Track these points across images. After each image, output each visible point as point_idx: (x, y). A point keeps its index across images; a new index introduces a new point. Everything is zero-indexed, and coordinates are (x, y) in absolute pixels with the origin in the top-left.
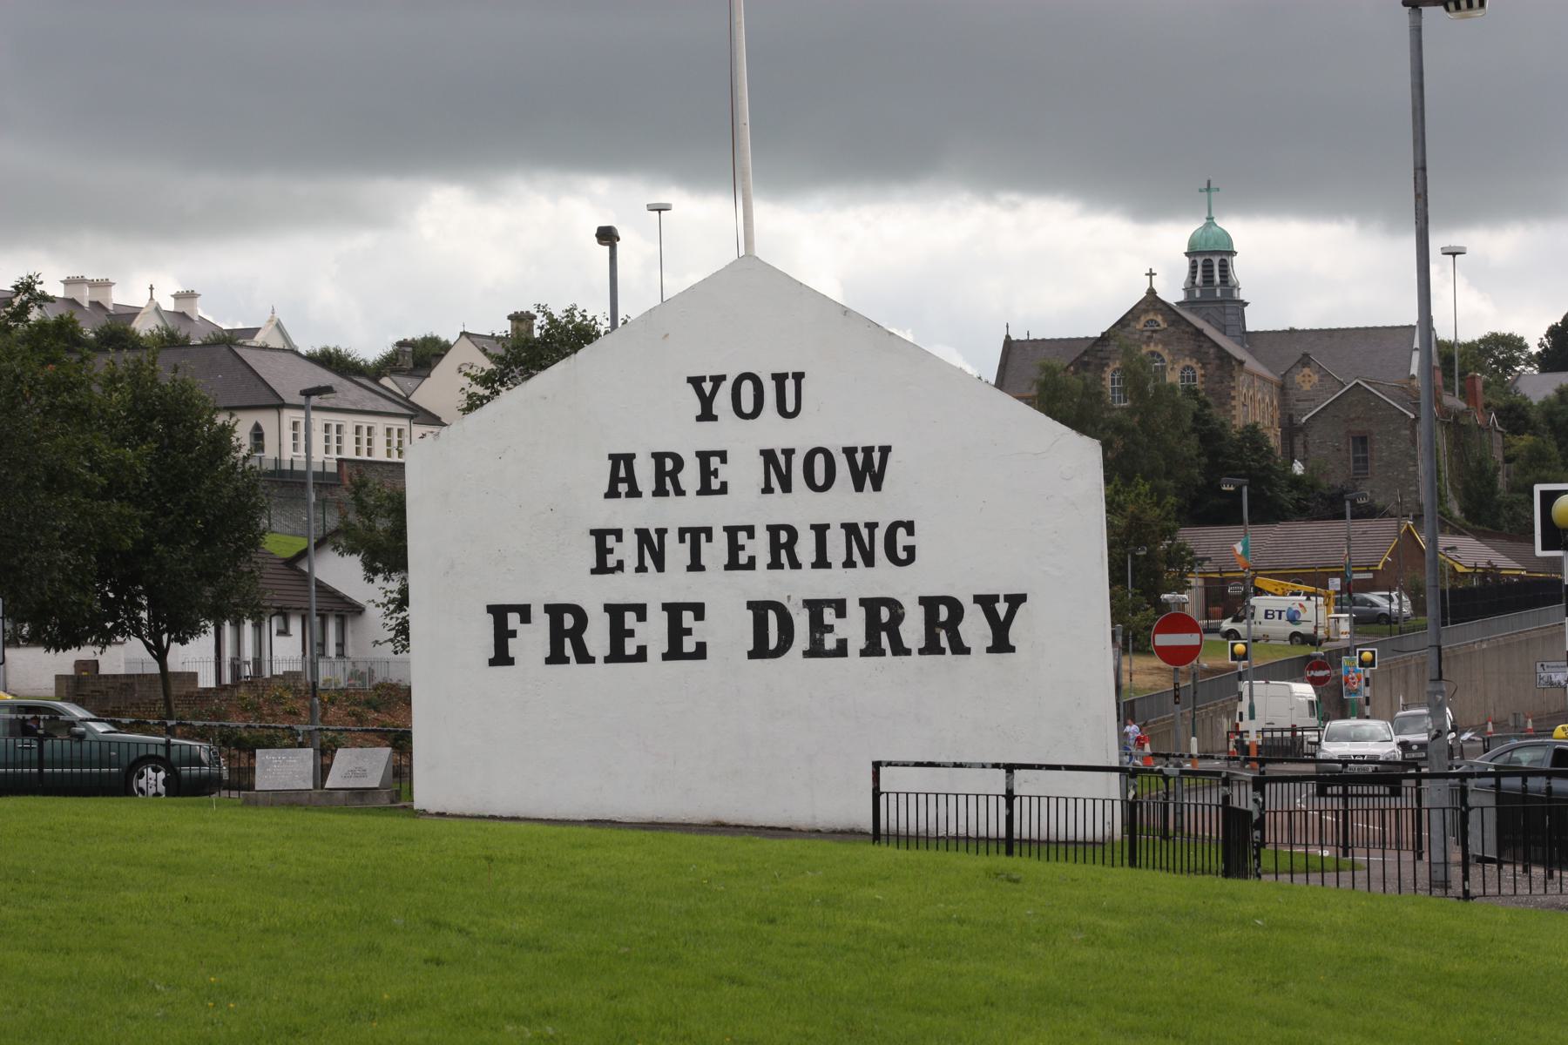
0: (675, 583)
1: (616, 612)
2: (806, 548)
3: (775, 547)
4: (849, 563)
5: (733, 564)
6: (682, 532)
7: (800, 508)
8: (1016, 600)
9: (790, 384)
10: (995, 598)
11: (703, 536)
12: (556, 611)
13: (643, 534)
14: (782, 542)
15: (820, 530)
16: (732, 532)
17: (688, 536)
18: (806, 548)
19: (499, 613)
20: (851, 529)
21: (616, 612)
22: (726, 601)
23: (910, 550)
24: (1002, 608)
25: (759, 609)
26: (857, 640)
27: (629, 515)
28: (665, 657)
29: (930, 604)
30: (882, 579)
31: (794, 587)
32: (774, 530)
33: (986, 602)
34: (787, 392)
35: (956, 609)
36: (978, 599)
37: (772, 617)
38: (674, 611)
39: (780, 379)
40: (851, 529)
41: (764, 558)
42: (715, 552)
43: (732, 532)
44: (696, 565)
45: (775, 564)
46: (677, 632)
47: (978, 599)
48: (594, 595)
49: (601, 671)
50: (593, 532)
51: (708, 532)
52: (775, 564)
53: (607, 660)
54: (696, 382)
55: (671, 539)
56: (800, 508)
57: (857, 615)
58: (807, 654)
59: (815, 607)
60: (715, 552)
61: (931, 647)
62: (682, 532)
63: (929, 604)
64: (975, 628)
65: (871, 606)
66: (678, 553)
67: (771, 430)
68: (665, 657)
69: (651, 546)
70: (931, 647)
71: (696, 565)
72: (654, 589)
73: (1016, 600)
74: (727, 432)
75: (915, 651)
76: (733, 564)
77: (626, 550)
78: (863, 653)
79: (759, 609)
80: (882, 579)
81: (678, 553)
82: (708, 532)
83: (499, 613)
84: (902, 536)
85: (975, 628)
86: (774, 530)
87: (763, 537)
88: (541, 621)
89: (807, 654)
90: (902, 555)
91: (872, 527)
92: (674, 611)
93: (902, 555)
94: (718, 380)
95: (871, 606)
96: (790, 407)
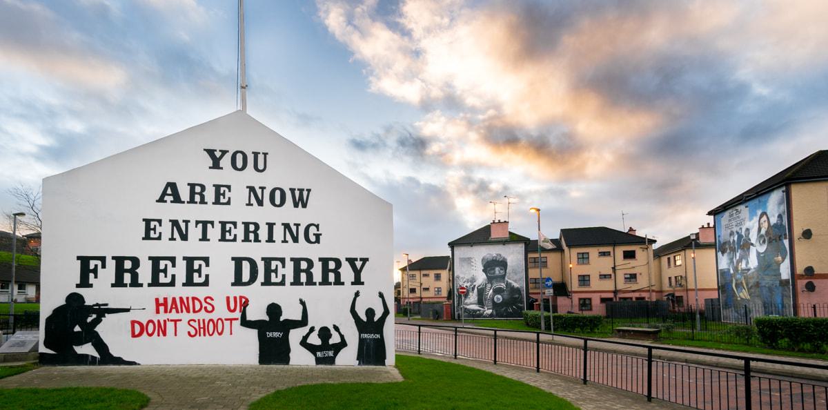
0: (193, 247)
1: (155, 261)
2: (263, 233)
3: (247, 232)
4: (285, 241)
5: (223, 239)
6: (197, 222)
7: (263, 215)
8: (365, 260)
9: (261, 158)
10: (356, 259)
11: (209, 226)
12: (119, 261)
13: (175, 223)
14: (251, 232)
15: (271, 226)
16: (223, 224)
17: (200, 226)
18: (263, 233)
19: (84, 261)
20: (287, 226)
21: (155, 261)
22: (221, 257)
23: (318, 236)
24: (359, 264)
25: (238, 261)
26: (290, 278)
27: (170, 211)
28: (184, 285)
29: (325, 261)
30: (302, 249)
31: (257, 251)
32: (246, 225)
33: (352, 261)
34: (259, 162)
35: (338, 263)
36: (347, 259)
37: (246, 267)
38: (190, 261)
39: (256, 154)
40: (287, 226)
41: (241, 236)
42: (214, 233)
43: (223, 224)
44: (204, 238)
45: (246, 239)
46: (190, 271)
47: (347, 259)
48: (144, 251)
49: (129, 289)
50: (144, 220)
51: (212, 223)
52: (246, 239)
53: (150, 285)
54: (211, 152)
55: (191, 225)
56: (263, 215)
57: (290, 265)
58: (263, 284)
59: (267, 261)
60: (214, 233)
61: (325, 282)
62: (197, 222)
63: (325, 261)
64: (347, 273)
65: (296, 262)
66: (195, 232)
67: (250, 176)
68: (184, 285)
69: (180, 230)
70: (325, 282)
71: (204, 238)
72: (180, 250)
73: (365, 260)
74: (226, 175)
75: (317, 284)
76: (223, 239)
77: (166, 229)
78: (292, 284)
79: (238, 261)
80: (302, 249)
81: (195, 232)
82: (212, 223)
83: (84, 261)
84: (313, 230)
85: (347, 273)
86: (246, 225)
87: (241, 228)
88: (111, 265)
89: (263, 284)
90: (313, 238)
91: (297, 225)
92: (190, 261)
93: (313, 238)
94: (224, 152)
95: (296, 262)
96: (261, 166)
